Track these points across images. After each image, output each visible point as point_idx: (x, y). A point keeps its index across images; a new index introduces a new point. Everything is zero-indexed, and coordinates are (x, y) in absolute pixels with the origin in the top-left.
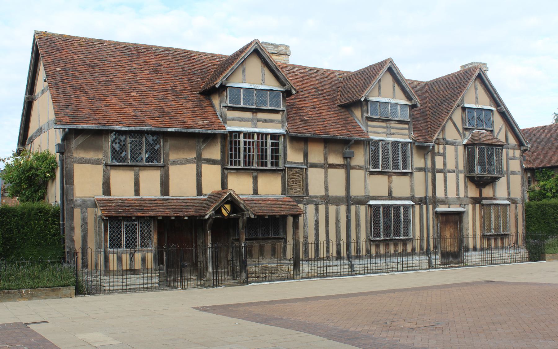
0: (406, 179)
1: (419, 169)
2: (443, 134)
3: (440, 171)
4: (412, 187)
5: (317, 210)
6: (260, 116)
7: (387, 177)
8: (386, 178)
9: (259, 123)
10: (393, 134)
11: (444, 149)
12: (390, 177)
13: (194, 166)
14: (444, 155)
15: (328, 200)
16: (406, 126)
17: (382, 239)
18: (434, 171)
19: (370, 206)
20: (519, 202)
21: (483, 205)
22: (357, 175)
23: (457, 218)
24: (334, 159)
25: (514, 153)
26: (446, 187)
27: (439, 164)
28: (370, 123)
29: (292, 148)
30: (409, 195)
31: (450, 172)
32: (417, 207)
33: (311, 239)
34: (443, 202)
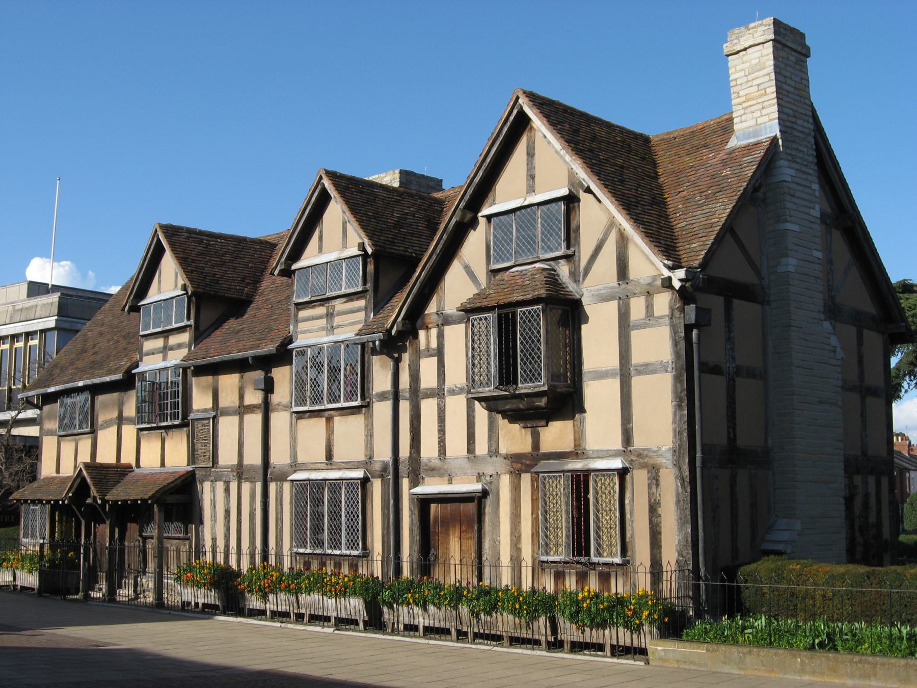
0: (357, 422)
1: (382, 396)
2: (440, 302)
3: (430, 394)
4: (370, 435)
5: (227, 490)
6: (173, 340)
7: (322, 422)
8: (319, 424)
9: (170, 353)
10: (338, 326)
11: (441, 336)
12: (329, 420)
13: (116, 427)
14: (440, 353)
15: (241, 472)
16: (361, 303)
17: (308, 551)
18: (416, 395)
19: (292, 481)
20: (662, 460)
21: (537, 473)
22: (280, 421)
23: (472, 507)
24: (254, 397)
25: (649, 307)
26: (442, 430)
27: (428, 379)
28: (302, 314)
29: (198, 386)
30: (362, 458)
31: (453, 392)
32: (377, 486)
33: (221, 544)
34: (433, 471)
